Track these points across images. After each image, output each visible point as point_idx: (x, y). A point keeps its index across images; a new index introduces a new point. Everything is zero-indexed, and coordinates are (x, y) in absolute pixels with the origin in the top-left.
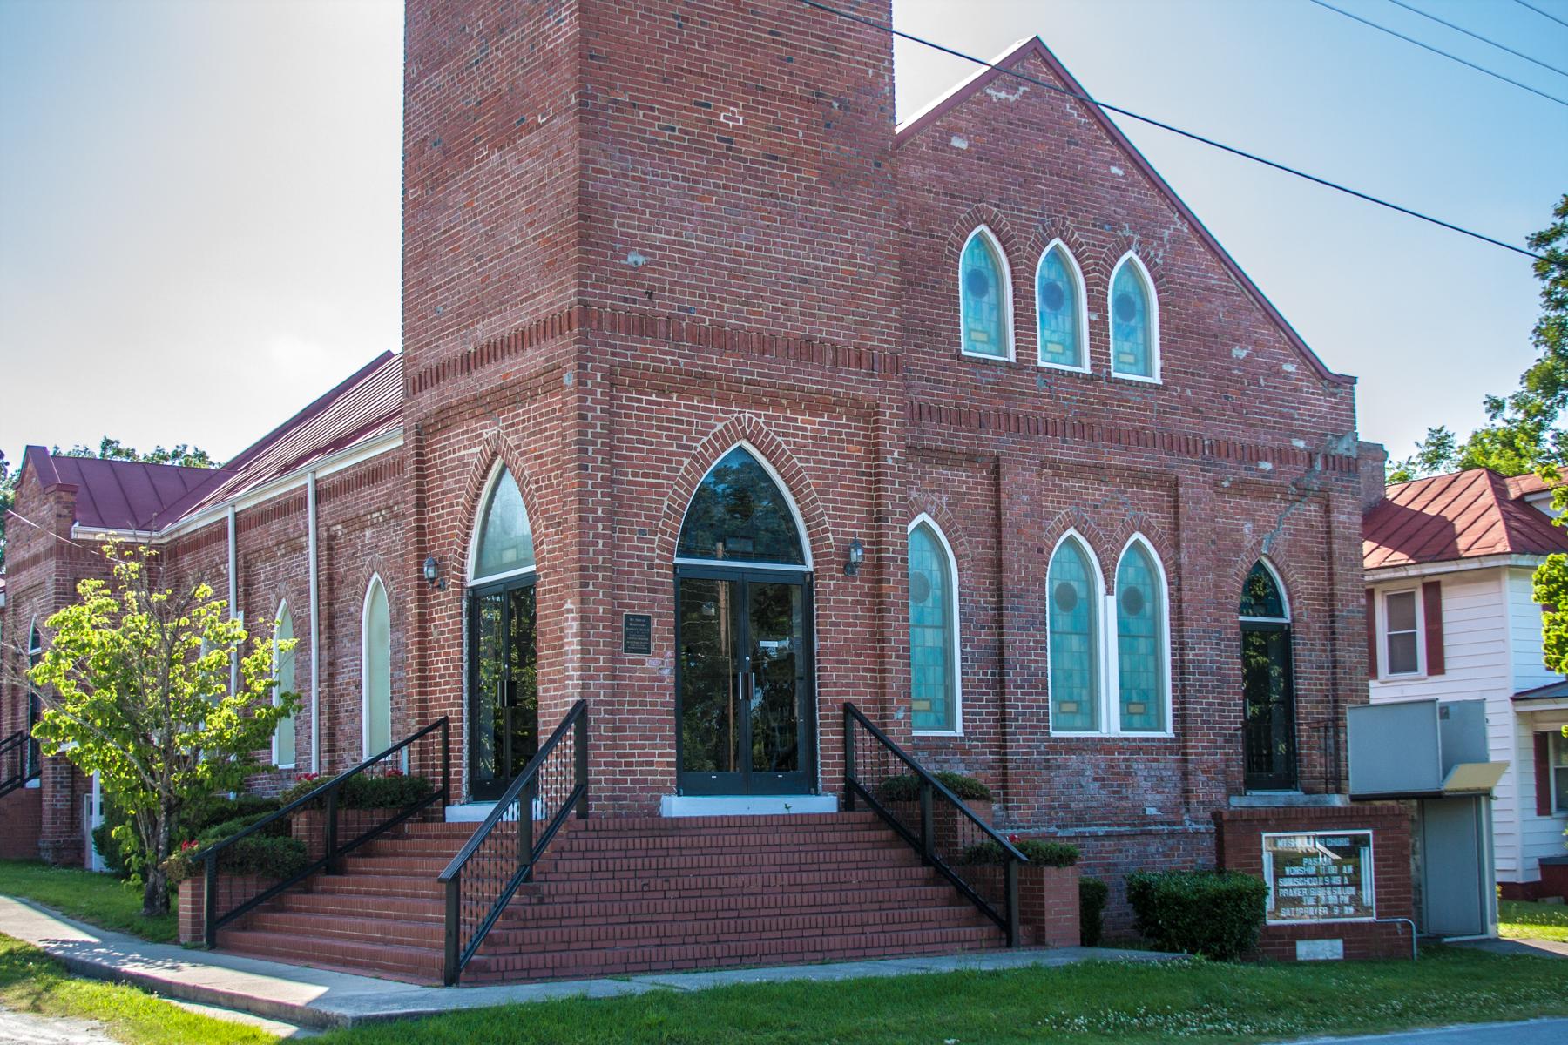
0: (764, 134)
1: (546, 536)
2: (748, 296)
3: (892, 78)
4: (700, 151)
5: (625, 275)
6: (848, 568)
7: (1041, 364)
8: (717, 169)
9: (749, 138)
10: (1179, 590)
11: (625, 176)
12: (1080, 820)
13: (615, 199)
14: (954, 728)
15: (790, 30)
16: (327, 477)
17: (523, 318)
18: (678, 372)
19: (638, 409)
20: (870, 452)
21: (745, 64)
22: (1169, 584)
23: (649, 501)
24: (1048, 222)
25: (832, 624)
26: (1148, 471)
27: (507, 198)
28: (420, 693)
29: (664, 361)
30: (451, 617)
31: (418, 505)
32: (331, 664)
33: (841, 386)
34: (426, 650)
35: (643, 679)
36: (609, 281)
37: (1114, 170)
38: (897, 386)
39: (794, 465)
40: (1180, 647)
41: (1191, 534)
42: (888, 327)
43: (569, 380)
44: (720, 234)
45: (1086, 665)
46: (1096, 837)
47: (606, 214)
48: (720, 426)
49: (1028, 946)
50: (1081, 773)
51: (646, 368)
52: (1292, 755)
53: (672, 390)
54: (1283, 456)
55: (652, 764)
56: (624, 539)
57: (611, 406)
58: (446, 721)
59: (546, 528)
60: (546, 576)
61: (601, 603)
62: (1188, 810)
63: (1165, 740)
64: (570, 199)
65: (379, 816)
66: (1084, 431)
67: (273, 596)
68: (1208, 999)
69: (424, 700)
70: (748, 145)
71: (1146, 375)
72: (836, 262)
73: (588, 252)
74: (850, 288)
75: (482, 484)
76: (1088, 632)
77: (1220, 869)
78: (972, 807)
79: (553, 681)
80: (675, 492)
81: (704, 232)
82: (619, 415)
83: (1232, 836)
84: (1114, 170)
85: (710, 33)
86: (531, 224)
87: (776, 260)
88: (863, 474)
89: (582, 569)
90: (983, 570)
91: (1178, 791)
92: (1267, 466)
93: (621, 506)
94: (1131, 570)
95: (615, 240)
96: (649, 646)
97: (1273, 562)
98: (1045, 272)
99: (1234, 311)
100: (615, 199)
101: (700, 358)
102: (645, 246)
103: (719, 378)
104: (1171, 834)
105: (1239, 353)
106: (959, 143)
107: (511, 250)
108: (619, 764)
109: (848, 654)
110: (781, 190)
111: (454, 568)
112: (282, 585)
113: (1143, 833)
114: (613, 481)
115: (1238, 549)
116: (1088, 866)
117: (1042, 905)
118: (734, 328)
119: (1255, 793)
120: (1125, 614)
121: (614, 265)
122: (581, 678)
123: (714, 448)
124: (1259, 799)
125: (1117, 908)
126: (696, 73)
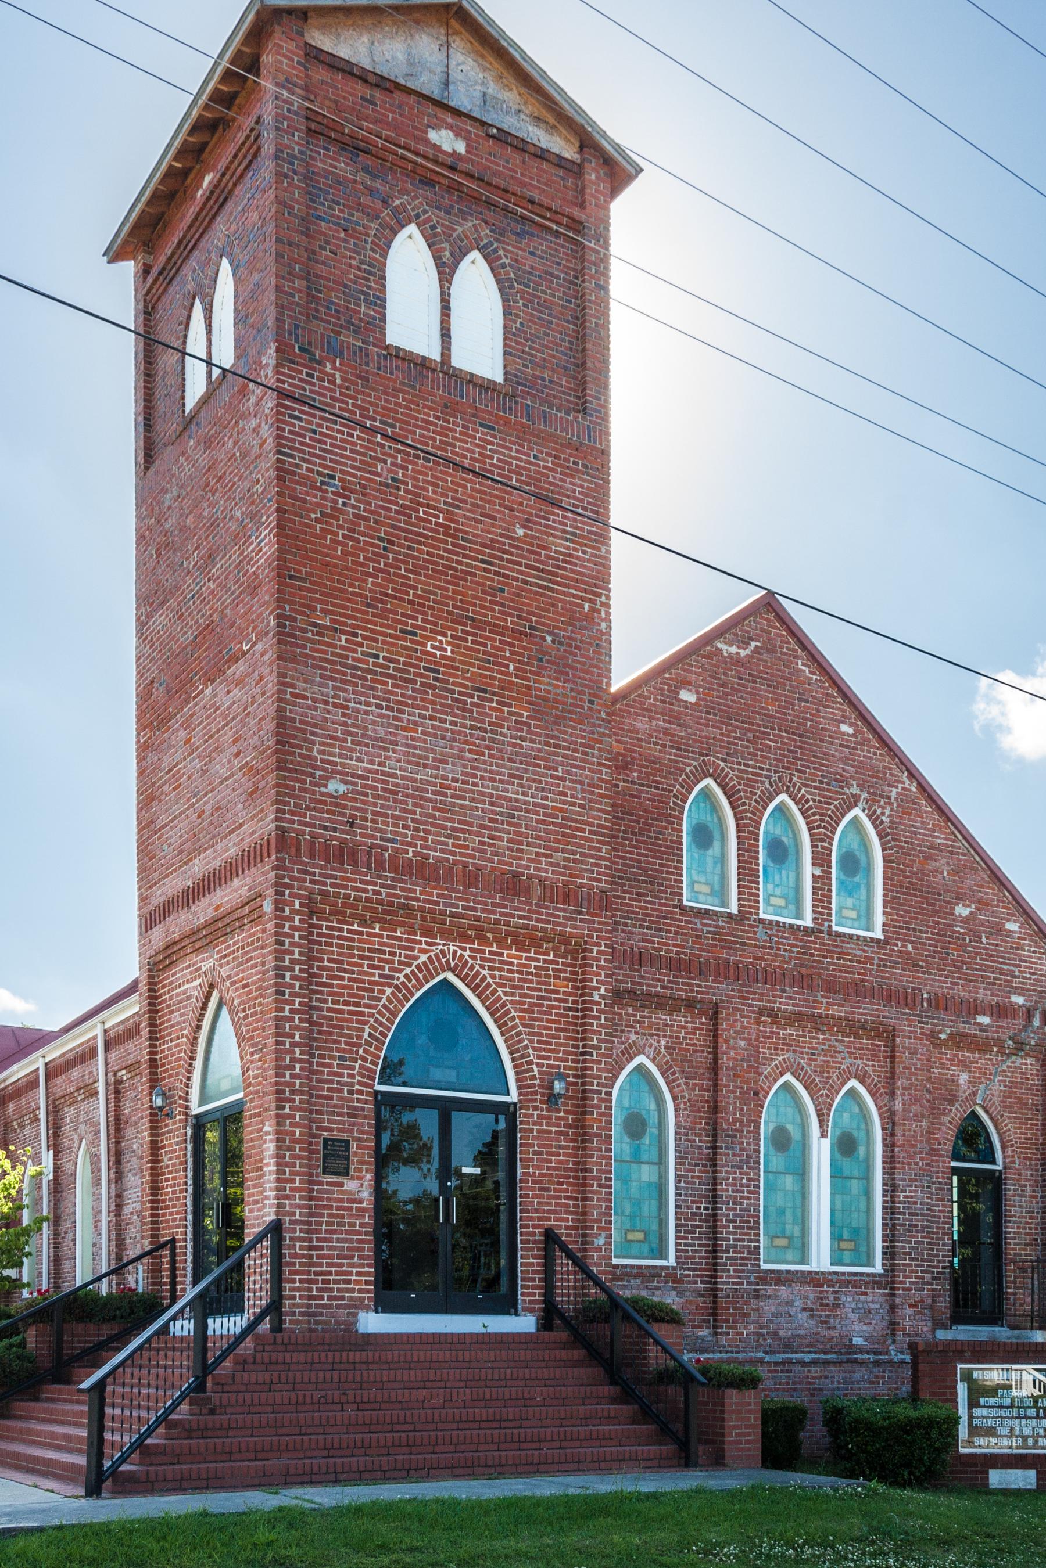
0: (473, 665)
1: (252, 1062)
2: (453, 829)
3: (608, 614)
4: (406, 680)
5: (325, 803)
6: (552, 1099)
7: (762, 916)
8: (422, 700)
9: (457, 669)
10: (893, 1135)
11: (326, 703)
12: (788, 1347)
13: (315, 726)
14: (666, 1258)
15: (502, 559)
16: (113, 1027)
17: (230, 849)
18: (380, 902)
19: (340, 938)
20: (577, 988)
21: (454, 592)
22: (883, 1129)
23: (349, 1028)
24: (775, 777)
25: (535, 1153)
26: (866, 1021)
27: (218, 731)
28: (152, 1215)
29: (366, 891)
30: (178, 1143)
31: (150, 1039)
32: (119, 1196)
33: (548, 922)
34: (158, 1175)
35: (342, 1201)
36: (308, 808)
37: (844, 728)
38: (605, 924)
39: (499, 998)
40: (891, 1189)
41: (907, 1083)
42: (599, 866)
43: (268, 907)
44: (425, 766)
45: (798, 1203)
46: (803, 1364)
47: (305, 740)
48: (423, 958)
49: (705, 1466)
50: (789, 1303)
51: (347, 896)
52: (999, 1293)
53: (375, 920)
54: (1001, 1011)
55: (349, 1282)
56: (323, 1065)
57: (311, 934)
58: (173, 1241)
59: (252, 1054)
60: (252, 1101)
61: (297, 1125)
62: (894, 1342)
63: (874, 1275)
64: (270, 725)
65: (107, 1330)
66: (804, 981)
67: (76, 1137)
68: (875, 1530)
69: (157, 1222)
70: (456, 676)
71: (868, 930)
72: (546, 798)
73: (285, 778)
74: (560, 825)
75: (202, 1015)
76: (802, 1173)
77: (914, 1397)
78: (659, 1330)
79: (256, 1202)
80: (376, 1020)
81: (409, 763)
82: (319, 943)
83: (931, 1365)
84: (844, 728)
85: (418, 558)
86: (237, 755)
87: (483, 794)
88: (570, 1009)
89: (278, 1092)
90: (699, 1111)
91: (885, 1323)
92: (985, 1020)
93: (320, 1032)
94: (846, 1115)
95: (315, 767)
96: (347, 1169)
97: (987, 1112)
98: (771, 827)
99: (958, 871)
100: (315, 726)
101: (402, 889)
102: (347, 774)
103: (422, 910)
104: (877, 1363)
105: (962, 911)
106: (688, 696)
107: (221, 783)
108: (316, 1282)
109: (551, 1182)
110: (490, 724)
111: (180, 1097)
112: (82, 1127)
113: (849, 1361)
114: (311, 1008)
115: (952, 1099)
116: (795, 1390)
117: (723, 1427)
118: (438, 860)
119: (961, 1327)
120: (838, 1156)
121: (314, 792)
122: (277, 1198)
123: (417, 979)
124: (962, 1333)
125: (814, 1433)
126: (402, 600)
